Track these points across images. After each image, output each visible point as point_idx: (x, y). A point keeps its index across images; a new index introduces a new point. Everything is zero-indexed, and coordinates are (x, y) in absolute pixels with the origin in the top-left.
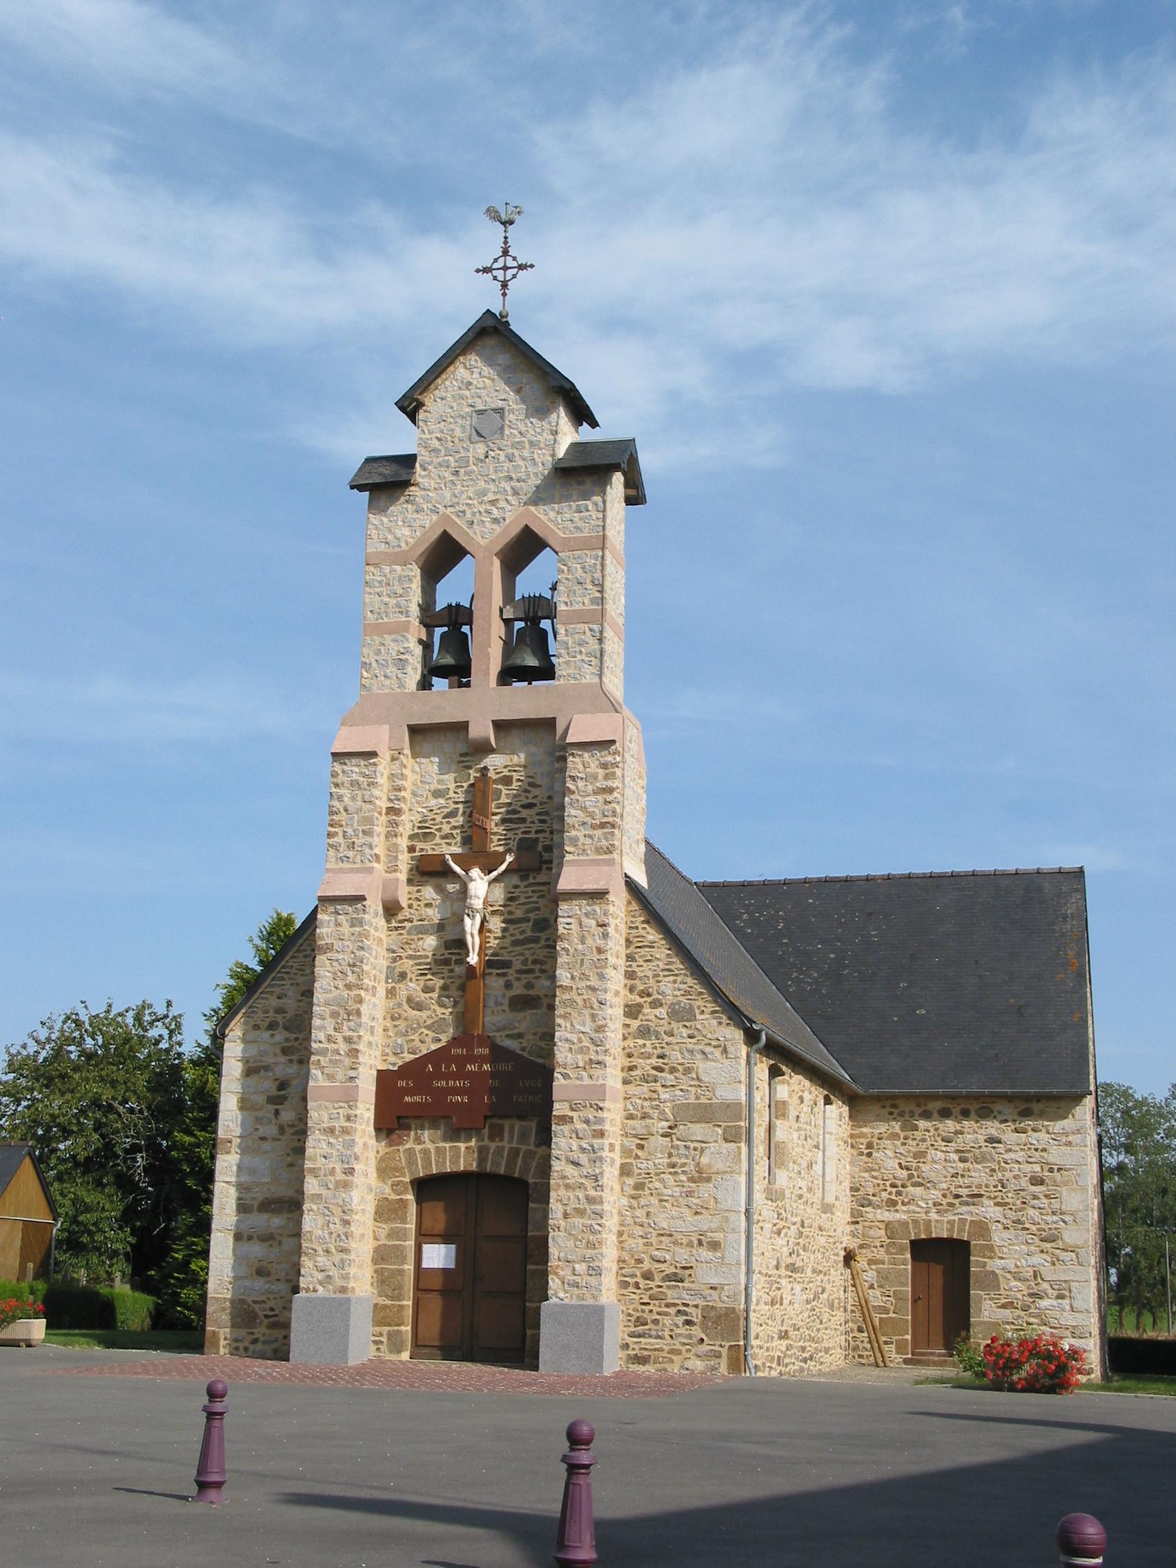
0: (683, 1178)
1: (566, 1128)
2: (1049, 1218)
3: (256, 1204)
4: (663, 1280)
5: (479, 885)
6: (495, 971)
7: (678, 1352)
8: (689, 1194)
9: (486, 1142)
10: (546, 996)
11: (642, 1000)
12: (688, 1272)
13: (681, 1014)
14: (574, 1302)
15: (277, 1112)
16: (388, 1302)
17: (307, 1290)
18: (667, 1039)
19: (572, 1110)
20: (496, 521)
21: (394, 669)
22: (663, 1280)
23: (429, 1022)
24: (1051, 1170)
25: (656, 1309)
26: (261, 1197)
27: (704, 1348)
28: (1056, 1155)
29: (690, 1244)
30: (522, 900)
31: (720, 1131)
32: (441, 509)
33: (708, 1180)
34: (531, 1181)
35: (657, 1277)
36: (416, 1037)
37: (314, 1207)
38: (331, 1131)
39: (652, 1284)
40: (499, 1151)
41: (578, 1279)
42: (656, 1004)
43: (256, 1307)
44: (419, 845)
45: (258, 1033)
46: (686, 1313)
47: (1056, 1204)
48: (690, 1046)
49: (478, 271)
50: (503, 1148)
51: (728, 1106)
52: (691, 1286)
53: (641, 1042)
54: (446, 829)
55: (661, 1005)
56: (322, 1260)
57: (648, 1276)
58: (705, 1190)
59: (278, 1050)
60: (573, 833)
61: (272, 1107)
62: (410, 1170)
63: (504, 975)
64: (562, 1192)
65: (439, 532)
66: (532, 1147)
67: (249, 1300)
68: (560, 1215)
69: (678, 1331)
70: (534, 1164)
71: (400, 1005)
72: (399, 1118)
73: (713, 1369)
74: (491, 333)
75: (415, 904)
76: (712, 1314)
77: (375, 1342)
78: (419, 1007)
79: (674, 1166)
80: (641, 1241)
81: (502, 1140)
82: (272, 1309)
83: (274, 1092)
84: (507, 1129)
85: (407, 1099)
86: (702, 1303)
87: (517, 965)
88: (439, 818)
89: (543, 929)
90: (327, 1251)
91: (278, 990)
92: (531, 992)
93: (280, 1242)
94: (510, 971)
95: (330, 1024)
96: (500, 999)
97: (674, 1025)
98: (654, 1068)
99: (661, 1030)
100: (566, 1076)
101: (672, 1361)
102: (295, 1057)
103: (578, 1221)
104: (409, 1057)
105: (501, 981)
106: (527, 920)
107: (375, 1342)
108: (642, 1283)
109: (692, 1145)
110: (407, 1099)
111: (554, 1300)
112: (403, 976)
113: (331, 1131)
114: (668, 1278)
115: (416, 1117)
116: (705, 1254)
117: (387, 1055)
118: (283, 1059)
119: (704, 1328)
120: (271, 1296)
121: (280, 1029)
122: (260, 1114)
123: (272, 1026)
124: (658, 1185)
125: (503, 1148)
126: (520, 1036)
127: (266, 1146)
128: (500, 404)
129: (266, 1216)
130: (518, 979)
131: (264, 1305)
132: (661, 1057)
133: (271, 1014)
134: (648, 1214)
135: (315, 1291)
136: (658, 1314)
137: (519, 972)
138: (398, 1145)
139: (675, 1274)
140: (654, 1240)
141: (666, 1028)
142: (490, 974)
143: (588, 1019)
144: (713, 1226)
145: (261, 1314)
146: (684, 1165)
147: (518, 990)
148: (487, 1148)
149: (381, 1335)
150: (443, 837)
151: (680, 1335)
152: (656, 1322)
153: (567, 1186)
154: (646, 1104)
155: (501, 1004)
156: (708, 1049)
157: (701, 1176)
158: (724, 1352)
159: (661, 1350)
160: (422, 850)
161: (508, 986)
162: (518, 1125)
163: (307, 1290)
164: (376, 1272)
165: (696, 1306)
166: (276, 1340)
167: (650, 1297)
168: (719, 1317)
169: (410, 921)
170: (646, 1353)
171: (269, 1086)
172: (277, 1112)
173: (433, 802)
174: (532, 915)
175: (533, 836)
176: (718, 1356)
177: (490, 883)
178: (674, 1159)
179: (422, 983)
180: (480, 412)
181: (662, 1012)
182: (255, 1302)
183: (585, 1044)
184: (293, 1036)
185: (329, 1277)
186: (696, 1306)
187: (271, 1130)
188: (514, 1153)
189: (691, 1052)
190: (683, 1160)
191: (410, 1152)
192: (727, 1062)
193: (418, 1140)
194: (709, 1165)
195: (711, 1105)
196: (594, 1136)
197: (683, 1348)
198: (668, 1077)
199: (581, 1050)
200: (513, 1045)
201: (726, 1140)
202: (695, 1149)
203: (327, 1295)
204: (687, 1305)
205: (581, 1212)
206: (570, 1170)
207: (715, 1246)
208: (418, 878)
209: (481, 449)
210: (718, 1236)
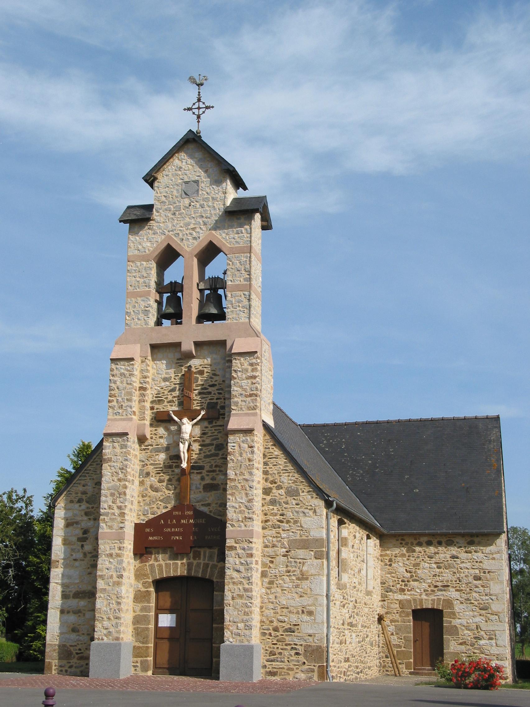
0: (294, 578)
1: (233, 553)
2: (484, 598)
3: (71, 594)
4: (284, 631)
5: (187, 427)
6: (196, 471)
7: (292, 669)
8: (297, 586)
9: (192, 560)
10: (222, 484)
11: (272, 486)
12: (297, 627)
13: (292, 493)
14: (238, 644)
15: (82, 546)
16: (141, 645)
17: (98, 639)
18: (285, 506)
19: (236, 543)
20: (195, 238)
21: (143, 315)
22: (284, 631)
23: (161, 498)
24: (484, 573)
25: (280, 647)
26: (74, 590)
27: (305, 667)
28: (487, 565)
29: (298, 613)
30: (210, 434)
31: (312, 553)
32: (167, 233)
33: (307, 579)
34: (215, 580)
35: (281, 630)
36: (155, 506)
37: (102, 595)
38: (111, 555)
39: (278, 634)
40: (198, 565)
41: (240, 631)
42: (279, 488)
43: (72, 648)
44: (156, 406)
45: (72, 504)
46: (296, 649)
47: (487, 590)
48: (297, 509)
49: (185, 109)
50: (200, 563)
51: (317, 540)
52: (299, 634)
53: (271, 507)
54: (170, 398)
55: (282, 488)
56: (106, 623)
57: (276, 629)
58: (305, 584)
59: (83, 513)
60: (236, 399)
61: (80, 544)
62: (152, 575)
63: (200, 473)
64: (231, 586)
65: (165, 244)
66: (215, 563)
67: (68, 645)
68: (230, 598)
69: (292, 658)
70: (216, 572)
71: (146, 489)
72: (146, 548)
73: (310, 678)
74: (192, 142)
75: (154, 437)
76: (310, 649)
77: (134, 666)
78: (156, 490)
79: (289, 572)
80: (272, 611)
81: (199, 559)
82: (80, 650)
83: (81, 535)
84: (202, 554)
85: (150, 538)
86: (304, 643)
87: (207, 468)
88: (166, 392)
89: (220, 450)
90: (109, 618)
91: (83, 482)
92: (215, 482)
93: (84, 615)
94: (204, 471)
95: (110, 500)
96: (198, 486)
97: (289, 498)
98: (278, 521)
99: (282, 501)
100: (232, 525)
101: (289, 674)
102: (92, 517)
103: (239, 601)
104: (151, 516)
105: (199, 476)
106: (212, 445)
107: (134, 666)
108: (273, 633)
109: (298, 561)
110: (150, 538)
111: (227, 643)
112: (148, 474)
113: (111, 555)
114: (286, 630)
115: (155, 548)
116: (305, 617)
117: (140, 515)
118: (85, 518)
119: (305, 657)
120: (80, 643)
121: (84, 502)
122: (74, 547)
123: (80, 501)
124: (281, 582)
125: (200, 563)
126: (209, 505)
127: (77, 564)
128: (197, 178)
129: (77, 600)
130: (208, 475)
131: (75, 648)
132: (282, 515)
133: (79, 495)
134: (276, 597)
135: (102, 639)
136: (282, 649)
137: (208, 471)
138: (146, 562)
139: (290, 628)
140: (279, 611)
141: (285, 500)
142: (193, 473)
143: (244, 496)
144: (310, 603)
145: (74, 652)
146: (294, 571)
147: (208, 481)
148: (192, 563)
149: (137, 662)
150: (169, 402)
151: (293, 660)
152: (280, 654)
153: (234, 583)
154: (274, 539)
155: (199, 488)
156: (306, 511)
157: (303, 577)
158: (316, 669)
159: (283, 668)
160: (157, 409)
161: (202, 479)
162: (208, 551)
163: (98, 639)
164: (134, 629)
165: (301, 645)
166: (82, 666)
167: (277, 641)
168: (313, 651)
169: (151, 445)
170: (275, 670)
171: (78, 532)
172: (82, 546)
173: (163, 384)
174: (215, 442)
175: (215, 401)
176: (313, 671)
177: (193, 426)
178: (289, 568)
179: (158, 478)
180: (186, 183)
181: (282, 492)
182: (71, 646)
183: (242, 509)
184: (90, 506)
185: (109, 632)
186: (301, 645)
187: (80, 555)
188: (206, 565)
189: (297, 512)
190: (294, 569)
191: (152, 566)
192: (316, 517)
193: (156, 560)
194: (307, 571)
195: (308, 540)
196: (247, 557)
197: (295, 667)
198: (286, 526)
199: (240, 512)
200: (205, 509)
201: (316, 558)
202: (300, 563)
203: (109, 641)
204: (296, 645)
205: (241, 597)
206: (235, 574)
207: (310, 613)
208: (155, 423)
209: (187, 201)
210: (312, 608)
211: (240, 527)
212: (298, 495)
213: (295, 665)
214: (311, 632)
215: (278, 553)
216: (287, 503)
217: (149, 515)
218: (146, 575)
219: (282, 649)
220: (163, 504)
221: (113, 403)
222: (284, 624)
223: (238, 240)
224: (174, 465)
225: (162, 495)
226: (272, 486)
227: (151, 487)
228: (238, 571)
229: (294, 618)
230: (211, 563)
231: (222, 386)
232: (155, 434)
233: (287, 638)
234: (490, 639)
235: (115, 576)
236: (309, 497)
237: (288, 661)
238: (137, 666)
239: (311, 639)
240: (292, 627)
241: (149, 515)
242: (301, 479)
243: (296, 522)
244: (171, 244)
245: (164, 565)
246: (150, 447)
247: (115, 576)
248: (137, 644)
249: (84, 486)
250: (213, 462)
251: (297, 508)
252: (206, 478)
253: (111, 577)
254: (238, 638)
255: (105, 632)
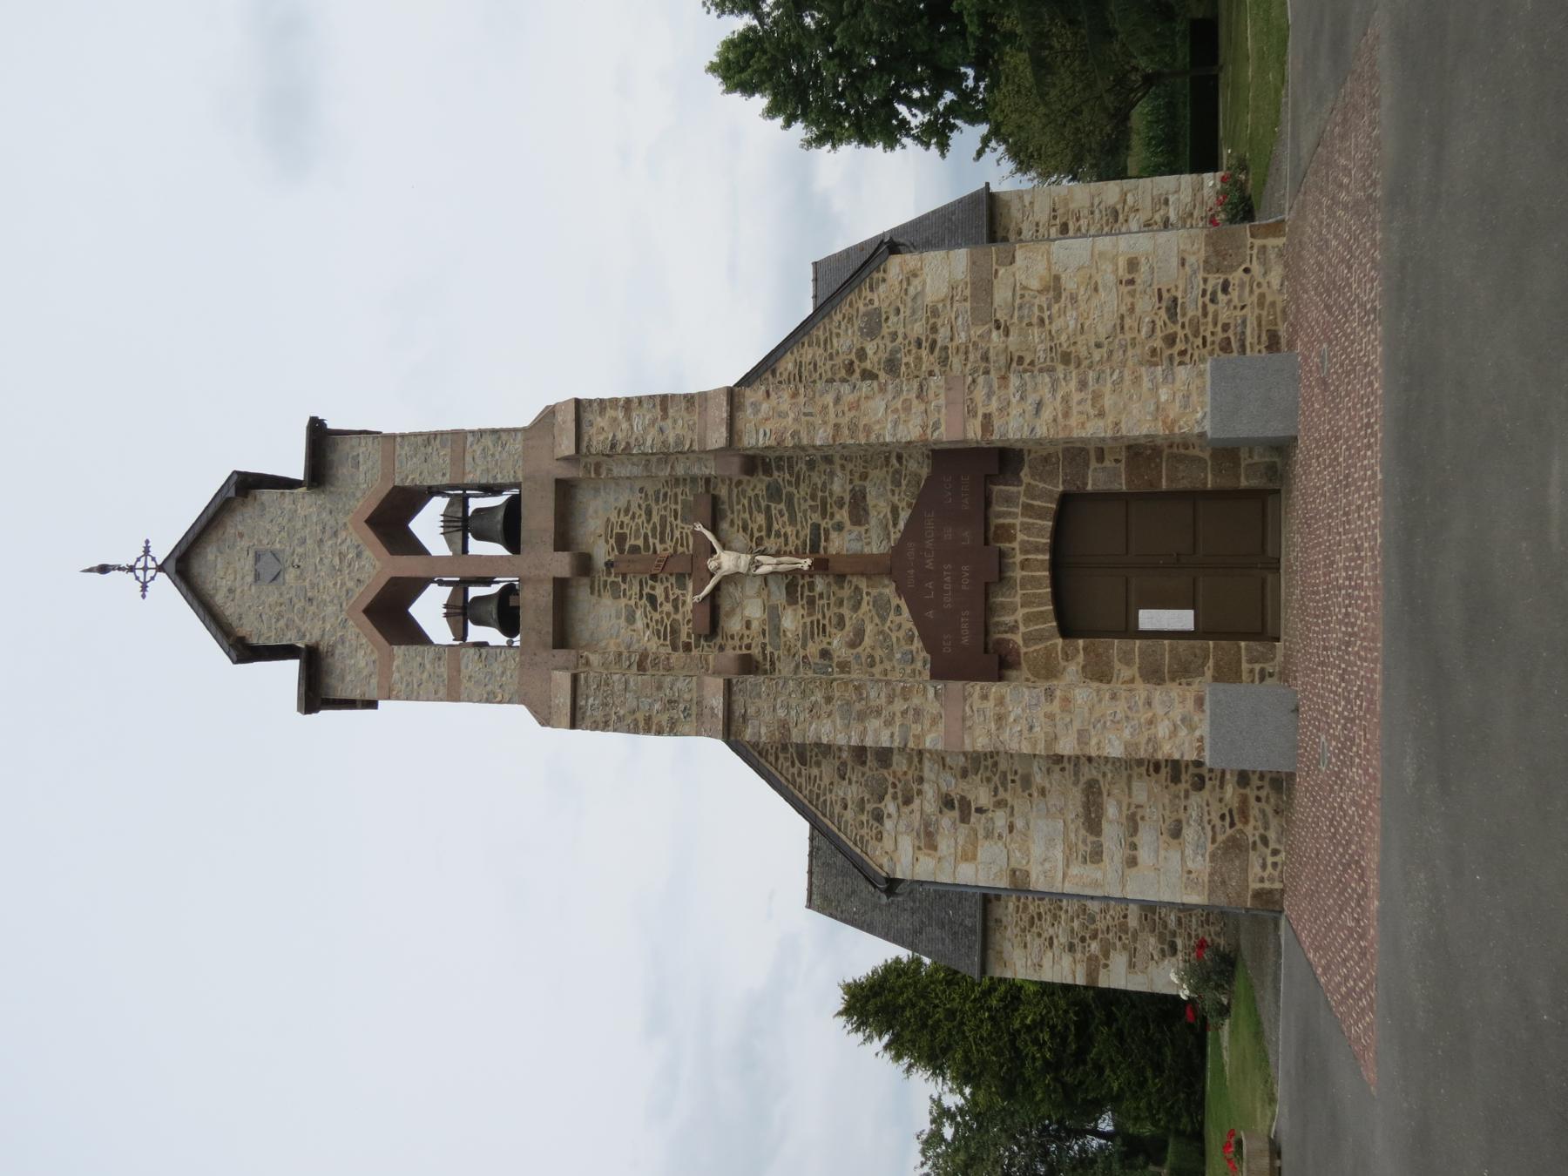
0: (1055, 308)
1: (997, 423)
2: (1097, 215)
3: (1091, 838)
4: (1175, 322)
5: (726, 561)
6: (823, 544)
7: (1262, 296)
8: (1074, 299)
9: (1016, 545)
10: (851, 481)
11: (858, 371)
12: (1165, 295)
13: (873, 325)
14: (1208, 399)
15: (979, 810)
16: (1211, 663)
17: (1200, 749)
18: (900, 339)
19: (975, 416)
20: (359, 555)
21: (496, 665)
22: (1175, 322)
23: (877, 620)
24: (1055, 218)
25: (1210, 328)
26: (1083, 832)
27: (1256, 268)
28: (1042, 215)
29: (1132, 294)
30: (747, 516)
31: (1001, 271)
32: (343, 616)
33: (1057, 278)
34: (1061, 488)
35: (1171, 329)
36: (894, 636)
37: (1094, 742)
38: (1000, 718)
39: (1181, 334)
40: (1026, 528)
41: (1179, 395)
42: (862, 354)
43: (1220, 838)
44: (684, 638)
45: (885, 835)
46: (1214, 293)
47: (1085, 212)
48: (908, 313)
49: (144, 596)
50: (1022, 524)
51: (974, 263)
52: (1181, 288)
53: (903, 368)
54: (668, 607)
55: (863, 349)
56: (1162, 730)
57: (1171, 340)
58: (1069, 284)
59: (906, 810)
60: (671, 440)
61: (974, 817)
62: (1048, 639)
63: (827, 531)
64: (1073, 421)
65: (364, 618)
66: (1022, 489)
67: (1210, 847)
68: (1101, 423)
69: (1236, 301)
70: (1041, 485)
71: (858, 656)
72: (986, 651)
73: (1280, 255)
74: (183, 565)
75: (746, 641)
76: (1214, 261)
77: (1262, 679)
78: (859, 634)
79: (1042, 321)
80: (1130, 353)
81: (1013, 526)
82: (1223, 817)
83: (956, 814)
84: (1001, 521)
85: (965, 641)
86: (1201, 275)
87: (816, 517)
88: (657, 616)
89: (779, 490)
90: (1151, 722)
91: (838, 809)
92: (847, 499)
93: (1138, 806)
94: (823, 525)
95: (874, 724)
96: (853, 536)
97: (885, 331)
98: (932, 350)
99: (890, 346)
100: (936, 426)
101: (1273, 304)
102: (915, 787)
103: (1108, 401)
104: (917, 644)
105: (834, 535)
106: (768, 507)
107: (1262, 679)
108: (1180, 346)
109: (1018, 301)
110: (965, 641)
111: (1207, 426)
112: (825, 654)
113: (1000, 718)
114: (1172, 315)
115: (987, 633)
116: (1142, 276)
117: (914, 671)
118: (917, 802)
119: (1232, 268)
120: (1206, 818)
121: (882, 806)
122: (981, 833)
123: (879, 817)
124: (1063, 338)
125: (1022, 524)
126: (895, 510)
127: (1019, 824)
128: (252, 554)
129: (1105, 825)
130: (832, 515)
131: (1218, 829)
132: (919, 345)
133: (864, 818)
134: (1098, 345)
135: (1201, 739)
136: (1215, 324)
137: (824, 515)
138: (1018, 654)
139: (1168, 309)
140: (1128, 336)
141: (887, 341)
142: (825, 549)
143: (871, 403)
144: (1110, 268)
145: (1229, 832)
146: (1041, 308)
147: (843, 515)
148: (1023, 542)
149: (1252, 671)
150: (676, 609)
151: (1240, 297)
152: (1226, 327)
153: (1066, 415)
154: (971, 357)
155: (860, 534)
156: (912, 291)
157: (1054, 286)
158: (1258, 242)
159: (1259, 318)
160: (689, 636)
161: (839, 527)
162: (997, 508)
163: (1200, 749)
164: (1173, 680)
165: (1205, 280)
166: (1263, 812)
167: (1196, 335)
168: (1217, 253)
169: (764, 649)
170: (1264, 337)
171: (947, 820)
172: (979, 810)
173: (639, 624)
174: (763, 504)
175: (679, 508)
176: (1263, 249)
177: (725, 547)
178: (1035, 320)
179: (834, 631)
180: (257, 577)
181: (870, 348)
182: (1214, 841)
183: (899, 405)
184: (891, 790)
185: (1183, 720)
186: (1205, 280)
187: (1000, 819)
188: (1028, 510)
189: (914, 312)
190: (1036, 309)
191: (1027, 639)
192: (926, 270)
193: (1013, 629)
194: (1041, 279)
195: (973, 284)
196: (1006, 387)
197: (1257, 291)
198: (943, 334)
199: (907, 408)
200: (904, 515)
201: (1012, 262)
202: (1022, 296)
203: (1207, 722)
204: (1204, 292)
205: (1097, 397)
206: (1047, 414)
207: (1133, 264)
208: (719, 640)
209: (290, 576)
210: (1122, 262)
211: (938, 408)
212: (878, 311)
213: (1251, 291)
214: (1175, 262)
215: (1002, 346)
216: (894, 336)
217: (914, 648)
218: (1049, 653)
219: (1215, 324)
220: (892, 616)
221: (664, 723)
222: (1159, 324)
223: (370, 463)
224: (806, 593)
225: (872, 619)
226: (858, 371)
227: (853, 645)
228: (1039, 406)
229: (1145, 304)
230: (1023, 499)
231: (651, 492)
232: (742, 638)
233: (1190, 314)
234: (1166, 202)
235: (1049, 708)
236: (882, 288)
237: (1243, 307)
238: (1262, 670)
239: (1191, 259)
240: (1164, 304)
241: (914, 648)
242: (845, 308)
243: (935, 313)
244: (364, 605)
245: (1026, 610)
246: (769, 649)
247: (1049, 708)
248: (1209, 673)
249: (845, 807)
250: (805, 506)
251: (905, 311)
252: (838, 517)
253: (1050, 717)
254: (1194, 398)
255: (1183, 732)
